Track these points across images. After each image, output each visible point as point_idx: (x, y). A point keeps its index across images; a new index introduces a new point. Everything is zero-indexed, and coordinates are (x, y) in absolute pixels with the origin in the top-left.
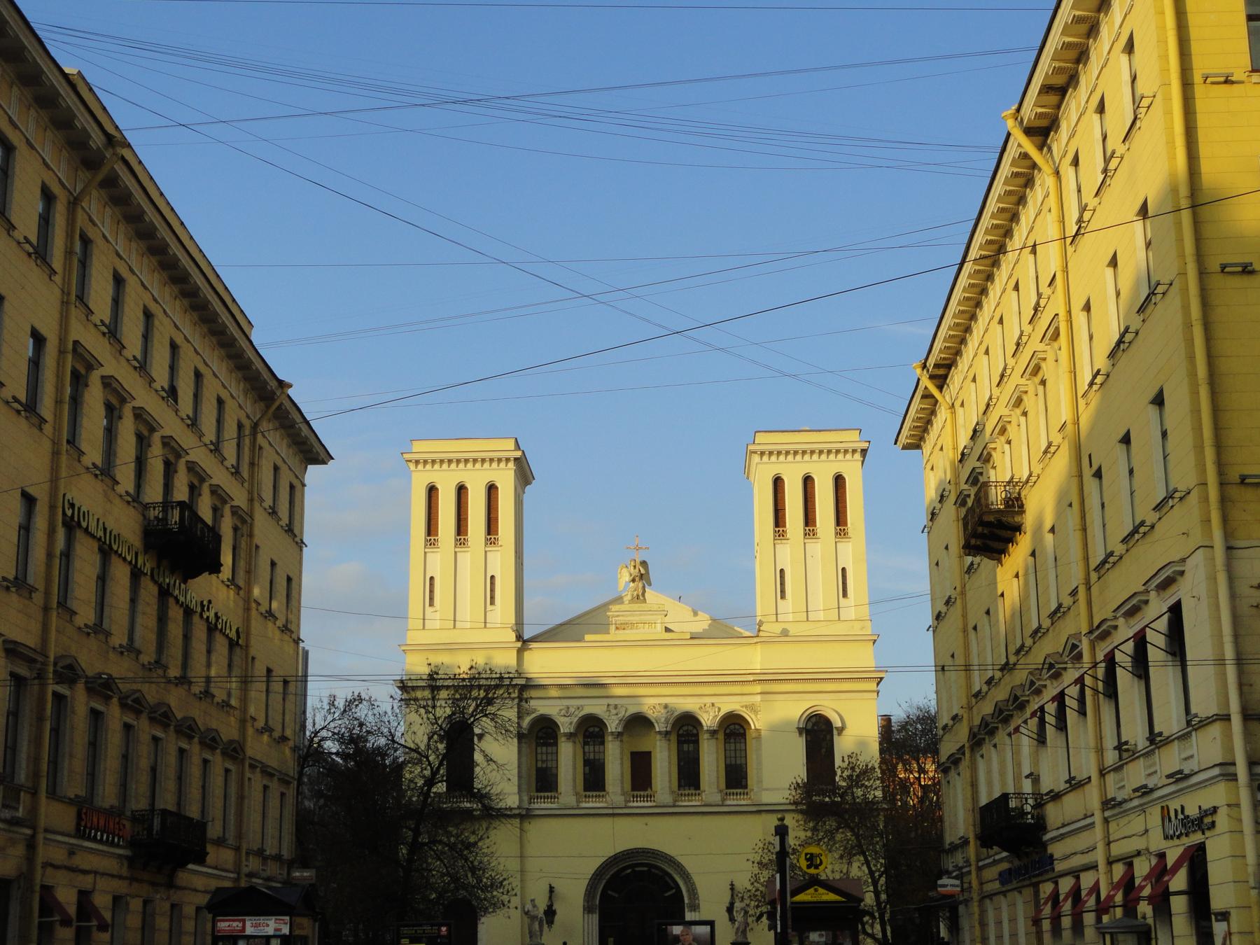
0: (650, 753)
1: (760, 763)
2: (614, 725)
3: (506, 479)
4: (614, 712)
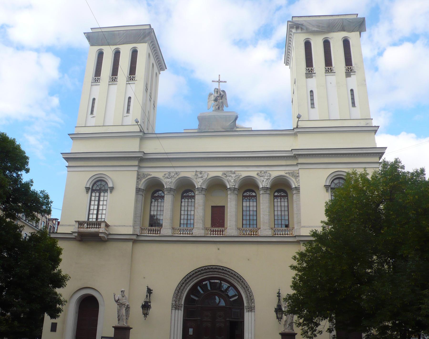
0: (224, 207)
1: (299, 210)
2: (200, 184)
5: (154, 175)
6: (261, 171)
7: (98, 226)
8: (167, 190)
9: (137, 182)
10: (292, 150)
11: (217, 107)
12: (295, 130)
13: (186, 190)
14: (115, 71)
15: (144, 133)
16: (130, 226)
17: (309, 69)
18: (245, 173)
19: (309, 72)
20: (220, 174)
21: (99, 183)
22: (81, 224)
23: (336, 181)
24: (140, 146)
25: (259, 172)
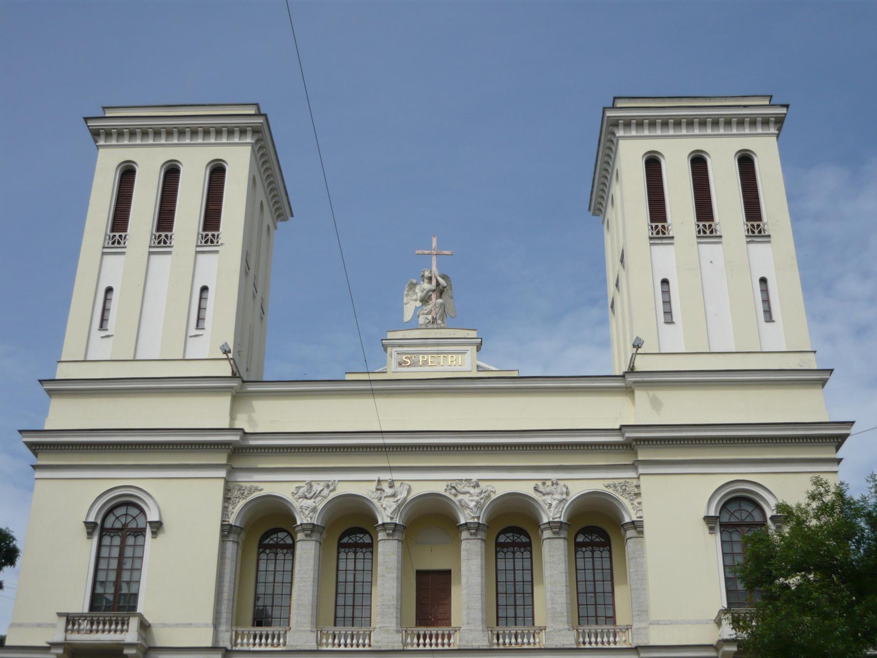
0: (446, 574)
2: (389, 511)
3: (239, 159)
4: (389, 491)
5: (268, 490)
6: (544, 481)
7: (119, 627)
8: (303, 530)
9: (225, 509)
10: (622, 426)
11: (430, 317)
12: (630, 379)
13: (351, 529)
14: (165, 219)
15: (244, 382)
16: (206, 625)
17: (657, 227)
18: (504, 484)
19: (658, 233)
20: (439, 488)
21: (121, 511)
22: (71, 620)
23: (733, 507)
24: (232, 417)
25: (540, 483)
